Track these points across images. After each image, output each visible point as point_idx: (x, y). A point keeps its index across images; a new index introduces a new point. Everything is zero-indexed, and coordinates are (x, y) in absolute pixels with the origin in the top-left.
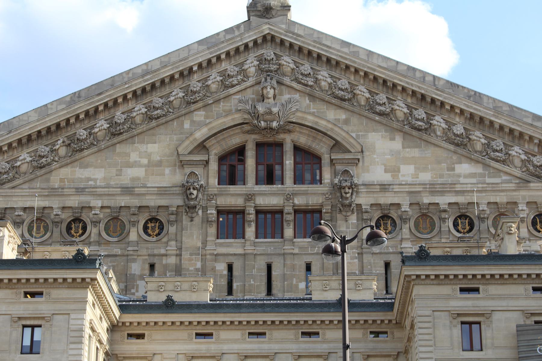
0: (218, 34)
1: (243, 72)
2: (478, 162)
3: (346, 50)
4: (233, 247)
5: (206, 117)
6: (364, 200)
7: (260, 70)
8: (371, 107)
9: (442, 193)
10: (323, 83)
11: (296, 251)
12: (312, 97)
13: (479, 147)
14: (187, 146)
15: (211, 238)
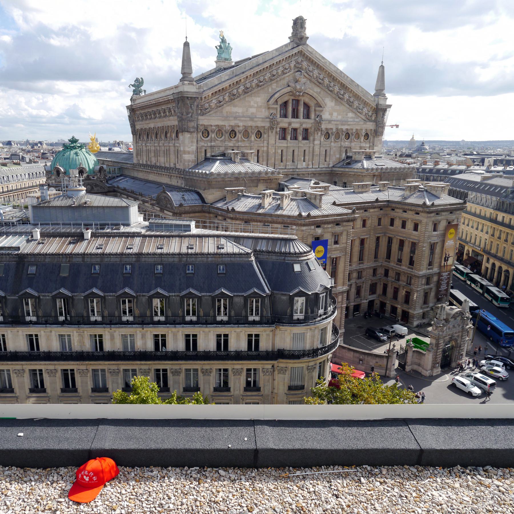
0: (282, 47)
1: (290, 67)
2: (354, 112)
3: (323, 61)
4: (283, 144)
5: (277, 87)
6: (323, 126)
7: (295, 66)
8: (328, 87)
9: (344, 125)
10: (315, 75)
11: (302, 145)
12: (310, 81)
13: (355, 107)
14: (273, 100)
15: (277, 140)
